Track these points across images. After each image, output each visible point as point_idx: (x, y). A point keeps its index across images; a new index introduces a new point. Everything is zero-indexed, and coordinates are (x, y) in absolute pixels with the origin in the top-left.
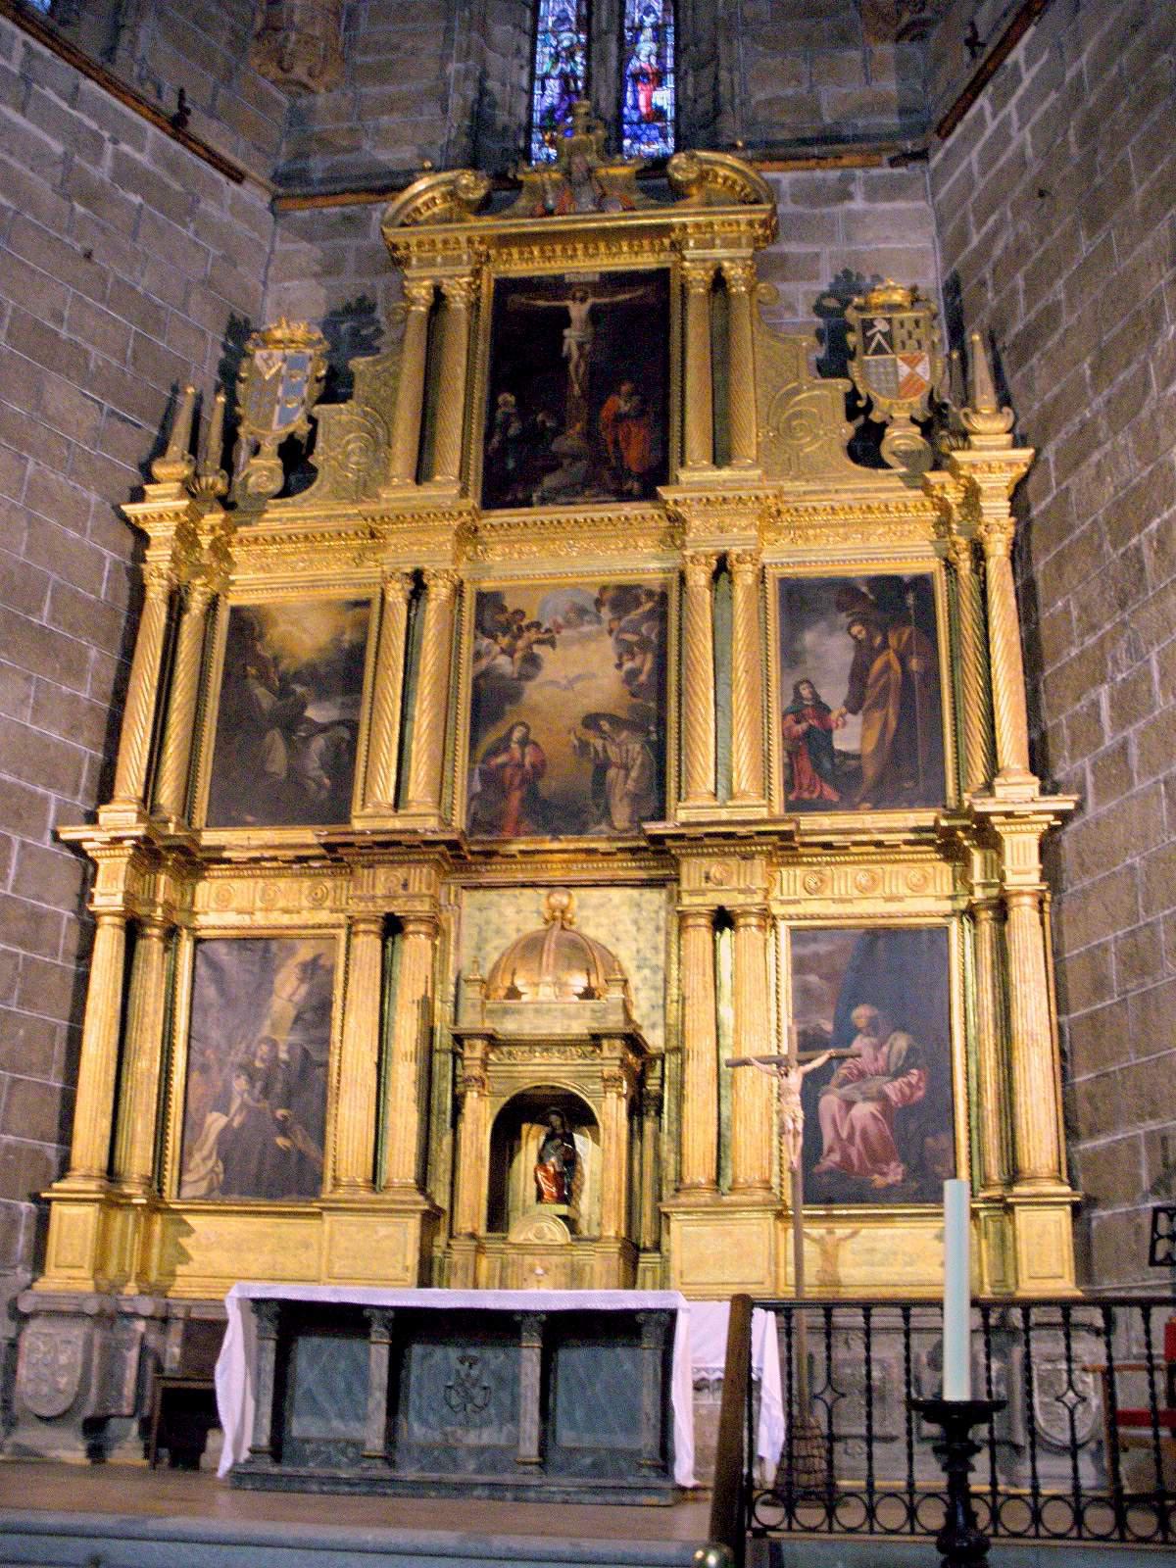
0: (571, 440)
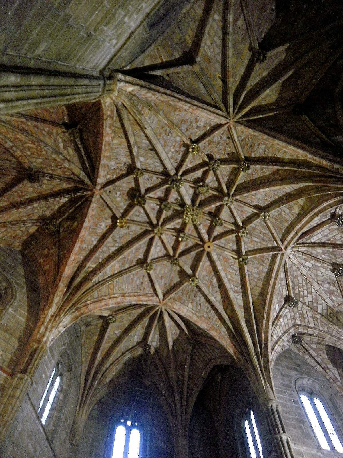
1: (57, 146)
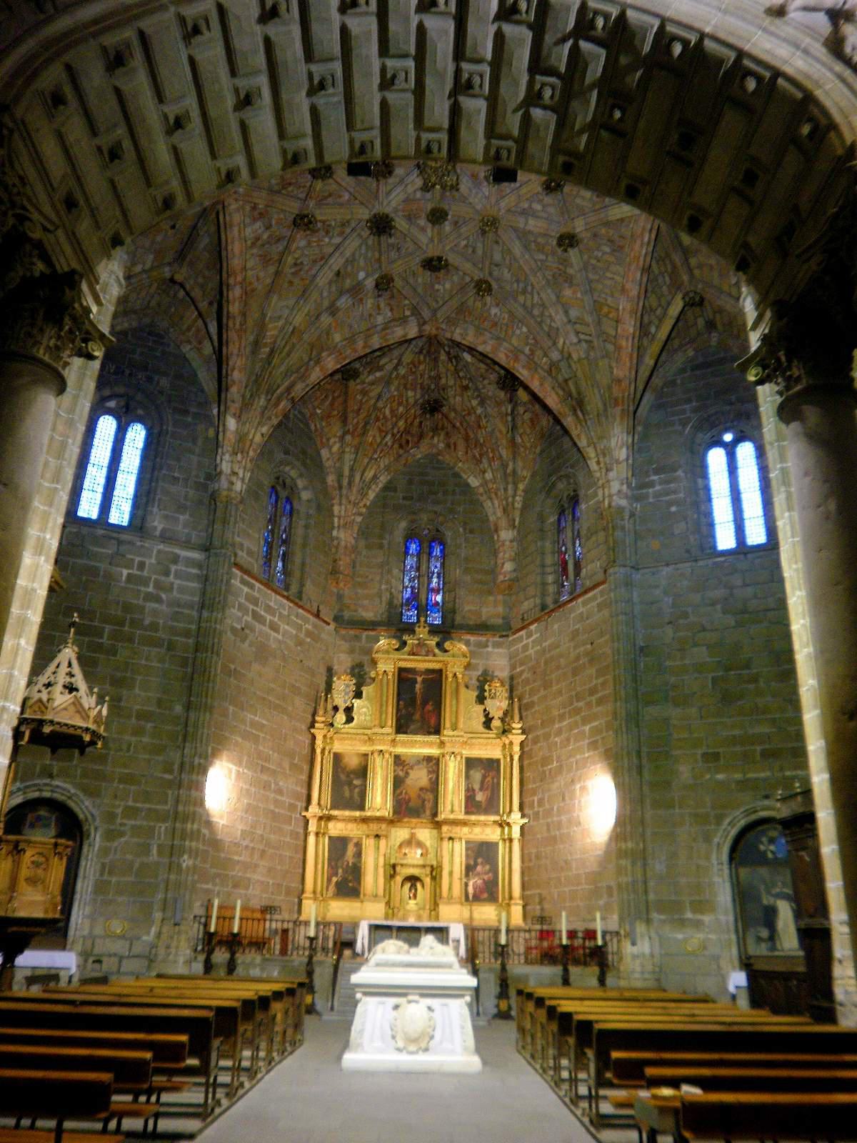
0: (417, 717)
1: (381, 378)
